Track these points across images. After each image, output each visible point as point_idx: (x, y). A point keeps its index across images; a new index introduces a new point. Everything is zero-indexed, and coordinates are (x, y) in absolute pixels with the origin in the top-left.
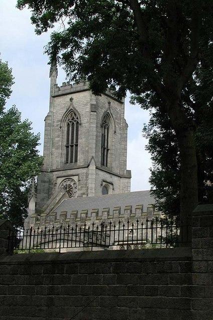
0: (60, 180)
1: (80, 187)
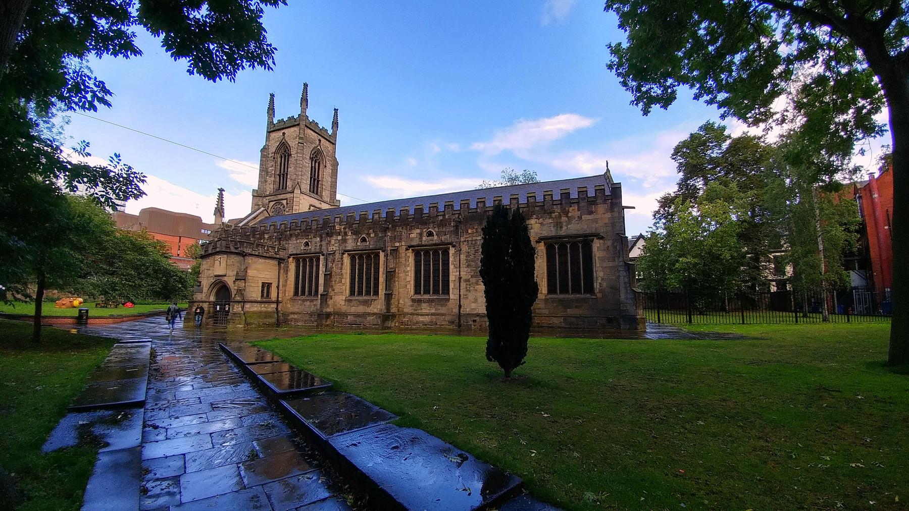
0: (272, 204)
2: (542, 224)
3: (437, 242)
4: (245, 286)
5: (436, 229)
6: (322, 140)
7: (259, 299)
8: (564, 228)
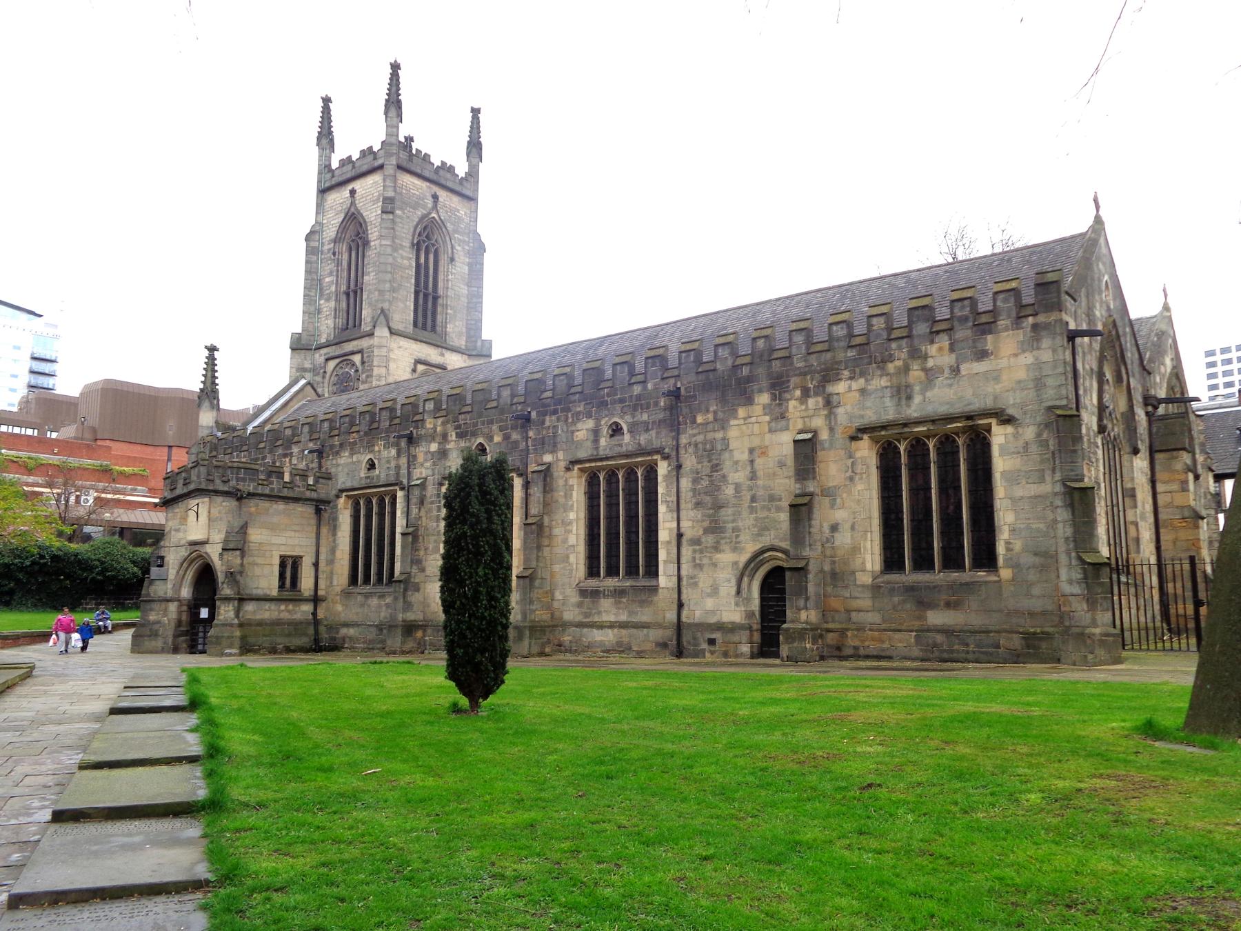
0: (332, 364)
1: (364, 376)
2: (863, 391)
3: (630, 448)
4: (242, 565)
5: (628, 418)
6: (443, 195)
7: (275, 593)
8: (917, 399)
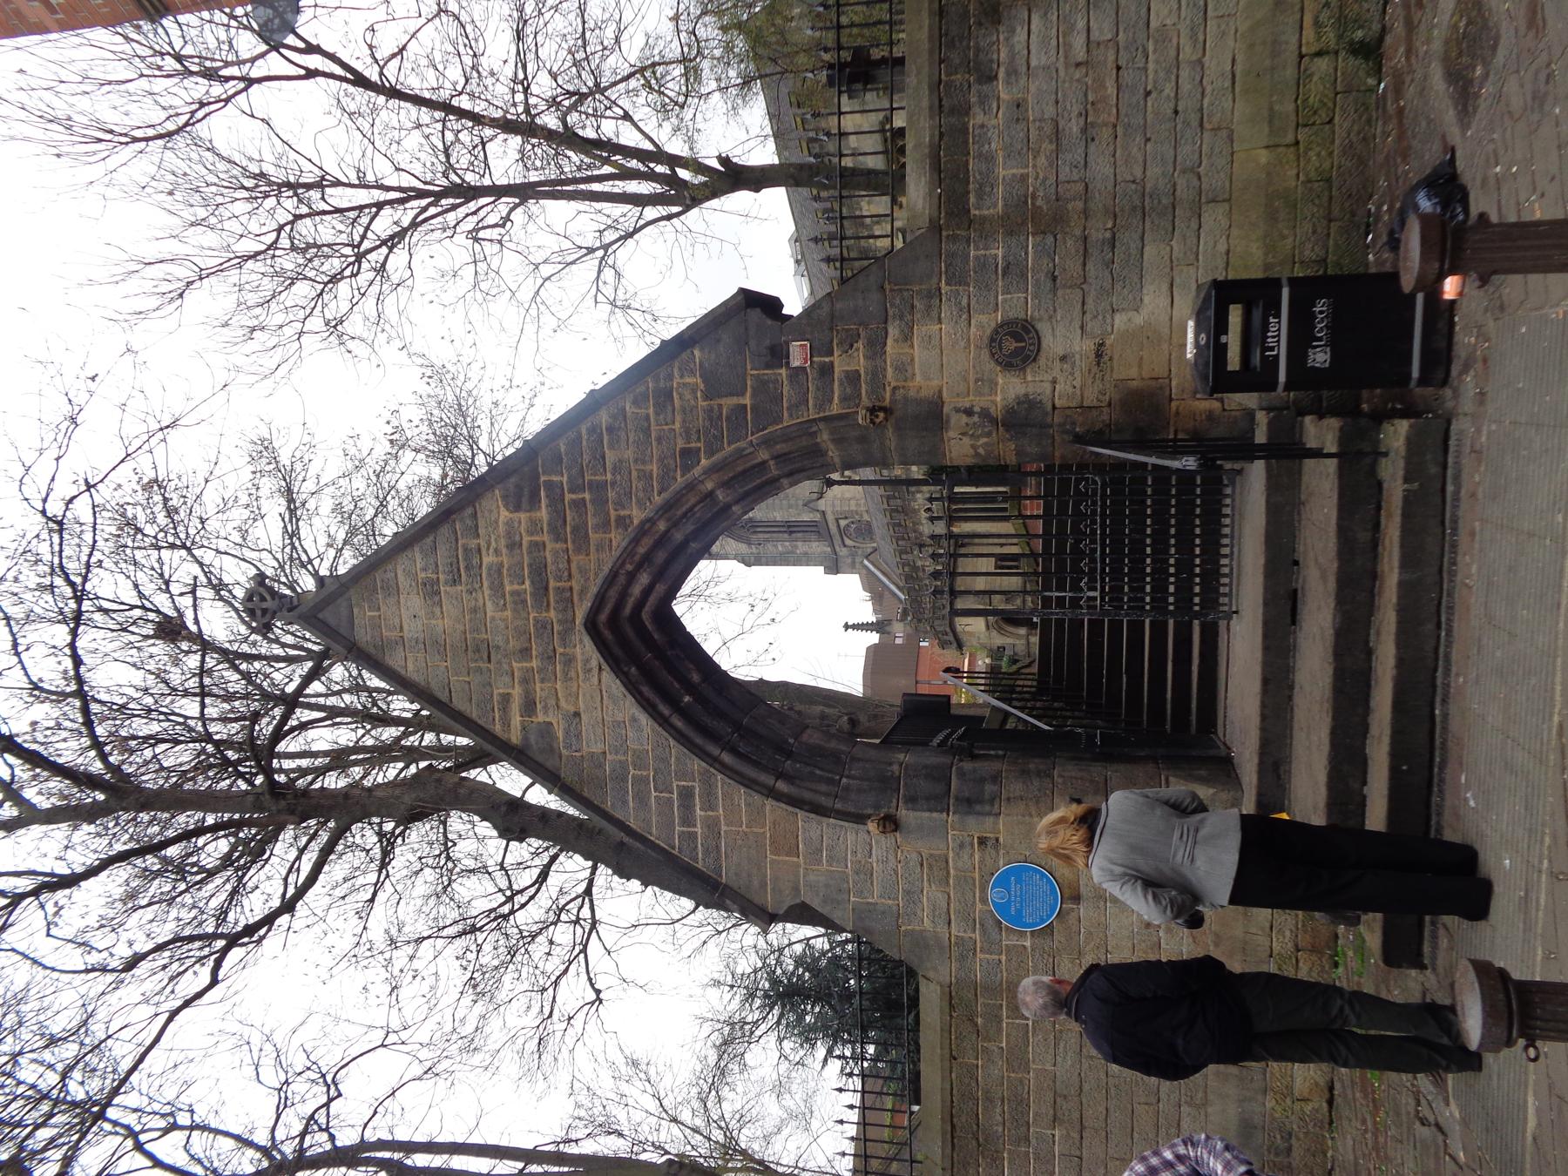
0: (848, 542)
